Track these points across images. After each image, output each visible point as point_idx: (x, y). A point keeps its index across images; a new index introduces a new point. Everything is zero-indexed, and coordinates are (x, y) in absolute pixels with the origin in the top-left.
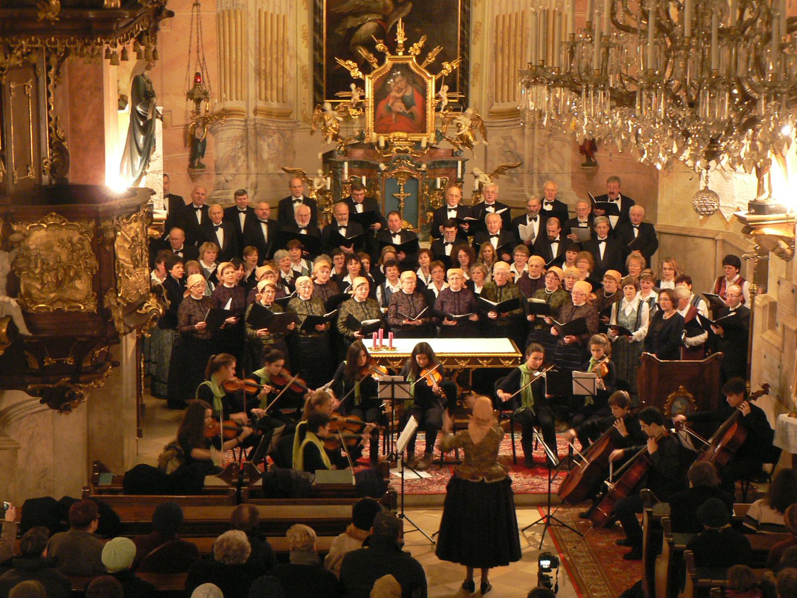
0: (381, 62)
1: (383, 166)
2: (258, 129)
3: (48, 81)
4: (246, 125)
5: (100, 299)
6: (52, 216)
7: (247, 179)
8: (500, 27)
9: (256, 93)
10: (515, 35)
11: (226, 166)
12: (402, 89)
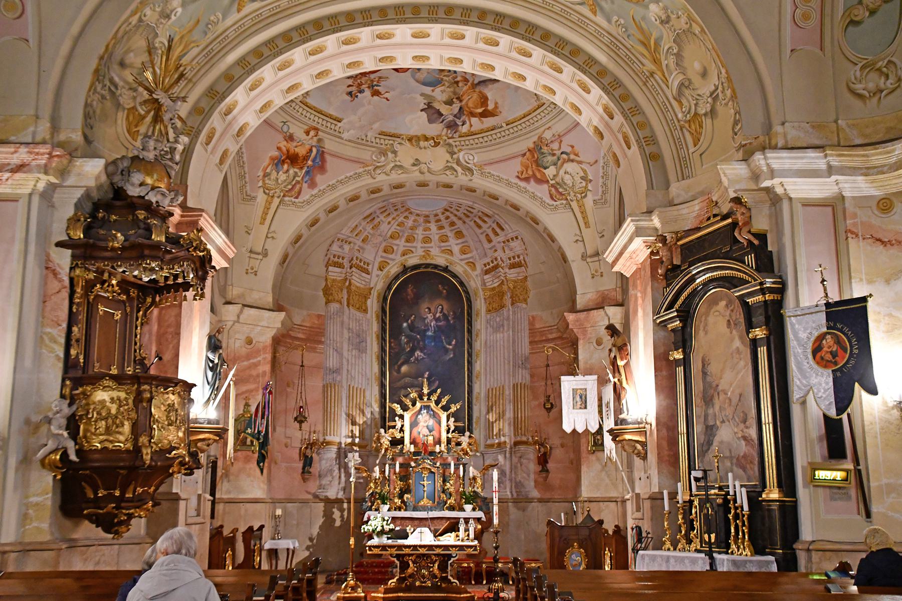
0: (414, 404)
1: (413, 464)
3: (137, 319)
5: (136, 440)
6: (106, 380)
7: (339, 484)
11: (326, 475)
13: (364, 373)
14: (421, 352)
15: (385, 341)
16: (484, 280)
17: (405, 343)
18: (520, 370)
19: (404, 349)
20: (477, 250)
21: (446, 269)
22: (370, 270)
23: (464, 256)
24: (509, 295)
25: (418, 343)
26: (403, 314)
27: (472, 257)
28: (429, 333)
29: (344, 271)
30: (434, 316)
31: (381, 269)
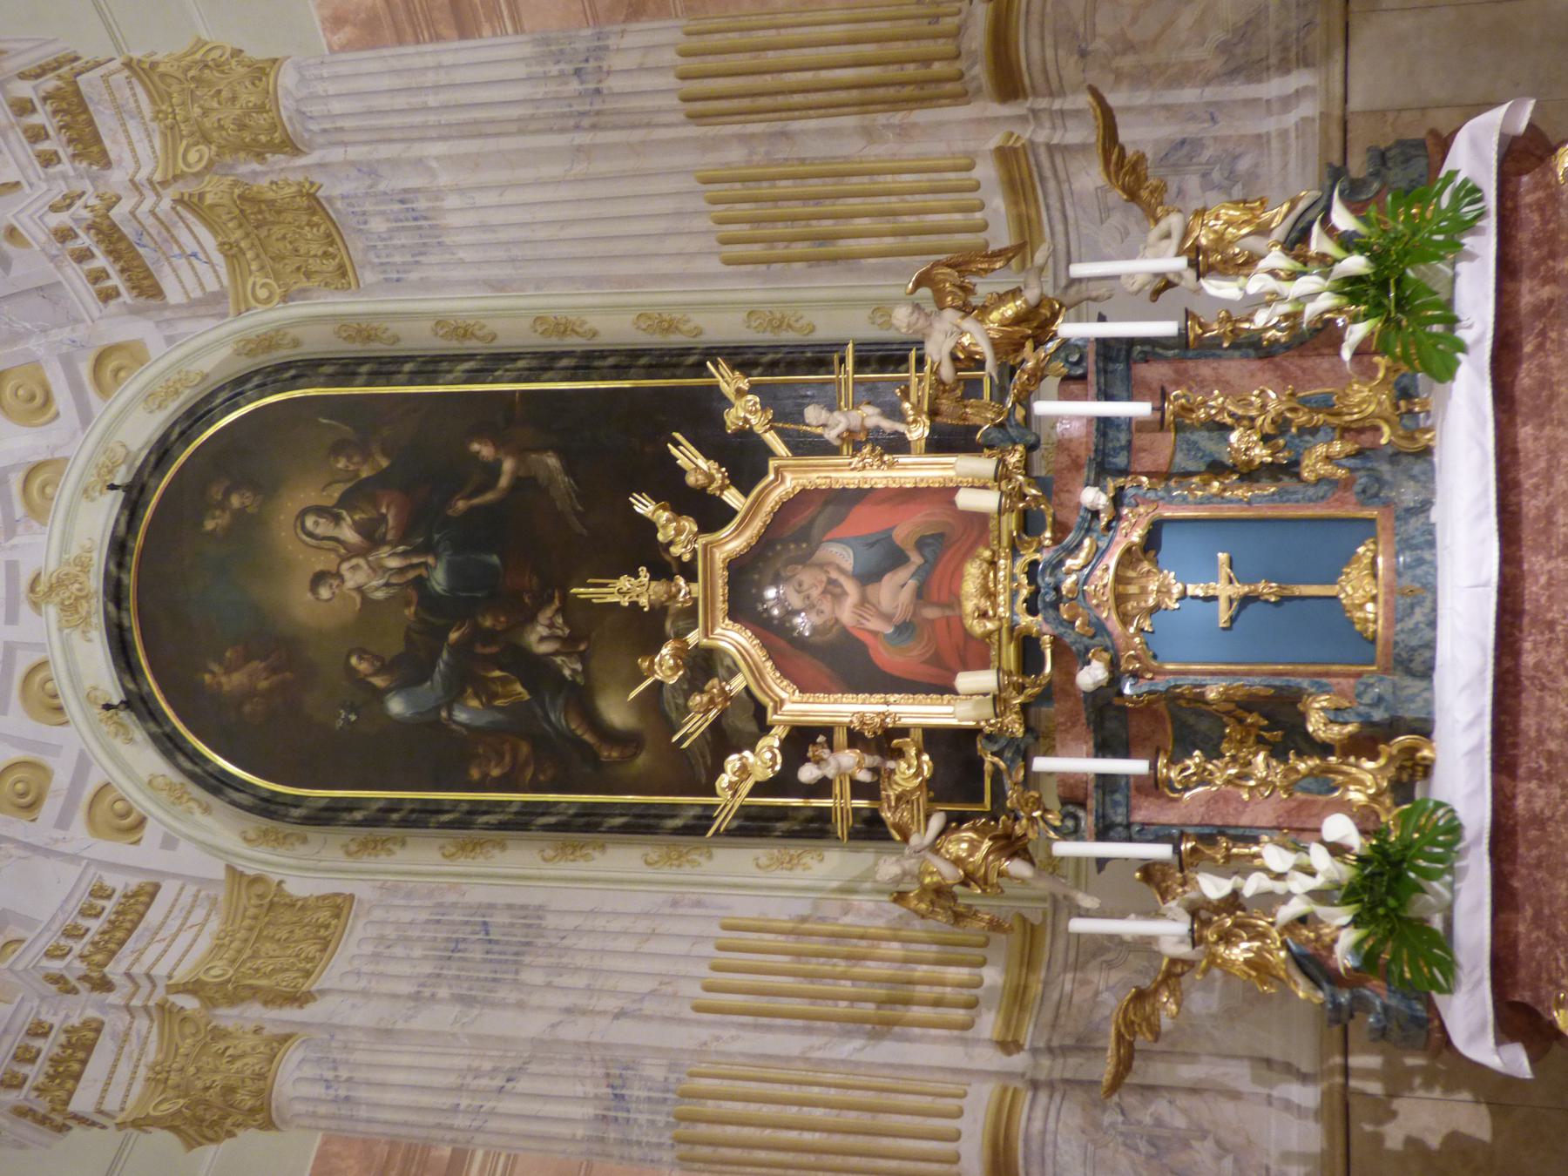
2: (1069, 1041)
4: (1051, 1085)
7: (1235, 1095)
8: (756, 250)
9: (948, 1040)
10: (776, 199)
12: (832, 582)
13: (642, 926)
14: (531, 619)
15: (476, 809)
16: (193, 304)
17: (488, 706)
18: (614, 84)
19: (516, 708)
20: (17, 337)
21: (134, 497)
22: (134, 882)
23: (63, 398)
24: (247, 167)
25: (490, 636)
26: (344, 718)
27: (68, 363)
28: (439, 579)
29: (115, 1022)
30: (352, 552)
31: (131, 826)
